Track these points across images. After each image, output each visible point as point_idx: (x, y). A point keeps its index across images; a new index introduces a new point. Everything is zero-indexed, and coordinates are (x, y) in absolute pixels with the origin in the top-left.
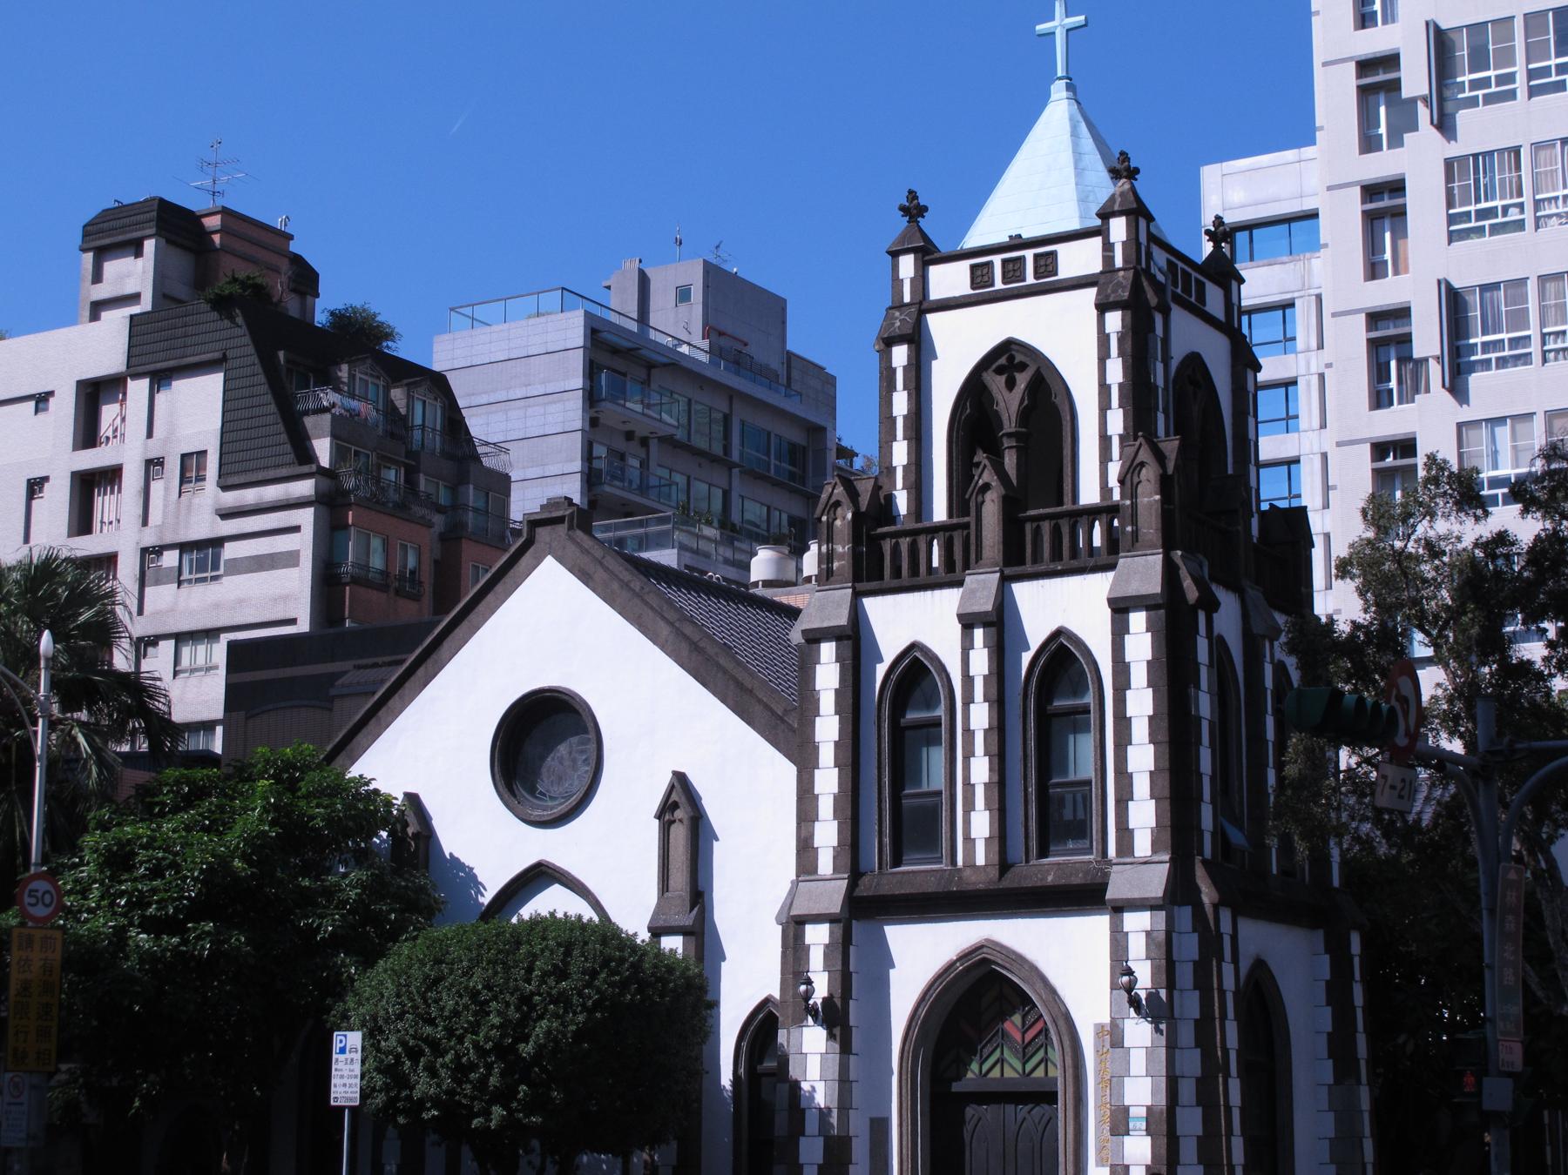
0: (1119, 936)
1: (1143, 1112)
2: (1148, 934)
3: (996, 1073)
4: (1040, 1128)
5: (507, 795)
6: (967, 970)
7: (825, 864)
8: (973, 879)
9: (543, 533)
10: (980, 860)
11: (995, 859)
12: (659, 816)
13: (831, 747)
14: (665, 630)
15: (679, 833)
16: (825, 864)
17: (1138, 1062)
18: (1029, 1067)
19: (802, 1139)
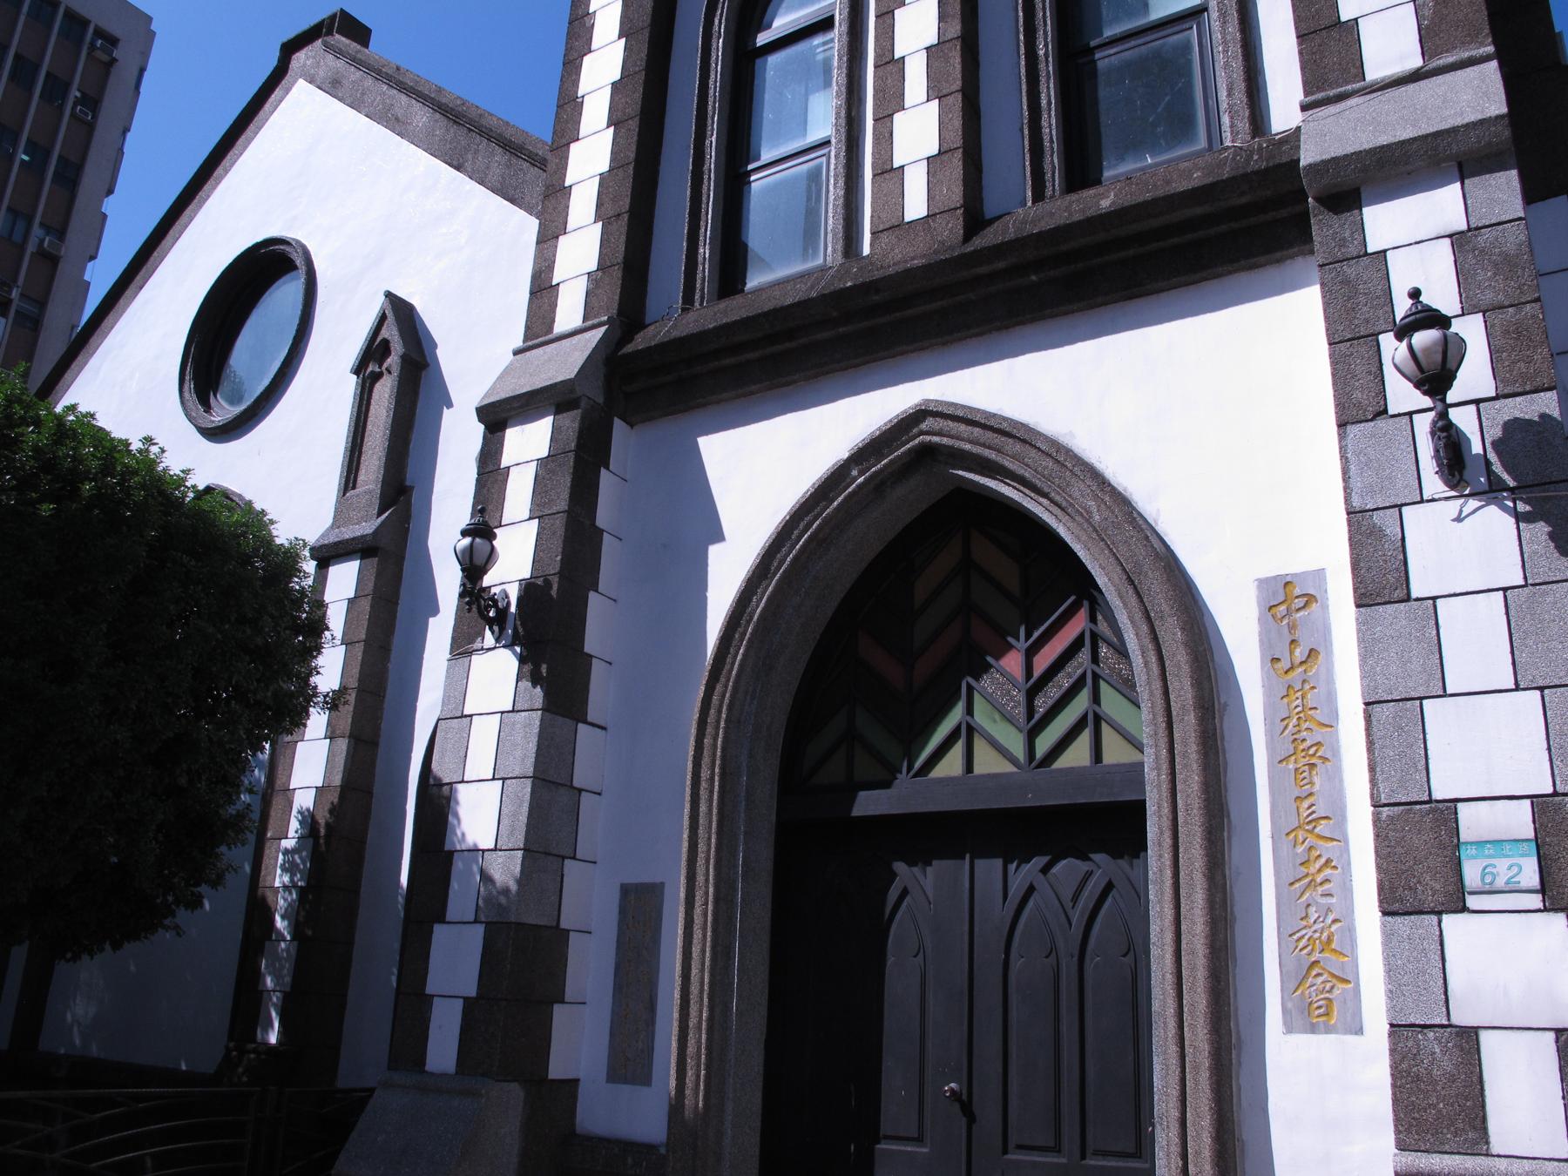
0: (1350, 270)
1: (1520, 820)
2: (1458, 240)
3: (951, 765)
4: (1078, 915)
5: (191, 397)
6: (878, 486)
7: (569, 311)
8: (897, 254)
9: (300, 59)
10: (916, 205)
11: (954, 194)
12: (358, 370)
13: (606, 93)
14: (421, 116)
15: (384, 391)
16: (569, 311)
17: (1475, 642)
18: (1044, 743)
19: (438, 930)
